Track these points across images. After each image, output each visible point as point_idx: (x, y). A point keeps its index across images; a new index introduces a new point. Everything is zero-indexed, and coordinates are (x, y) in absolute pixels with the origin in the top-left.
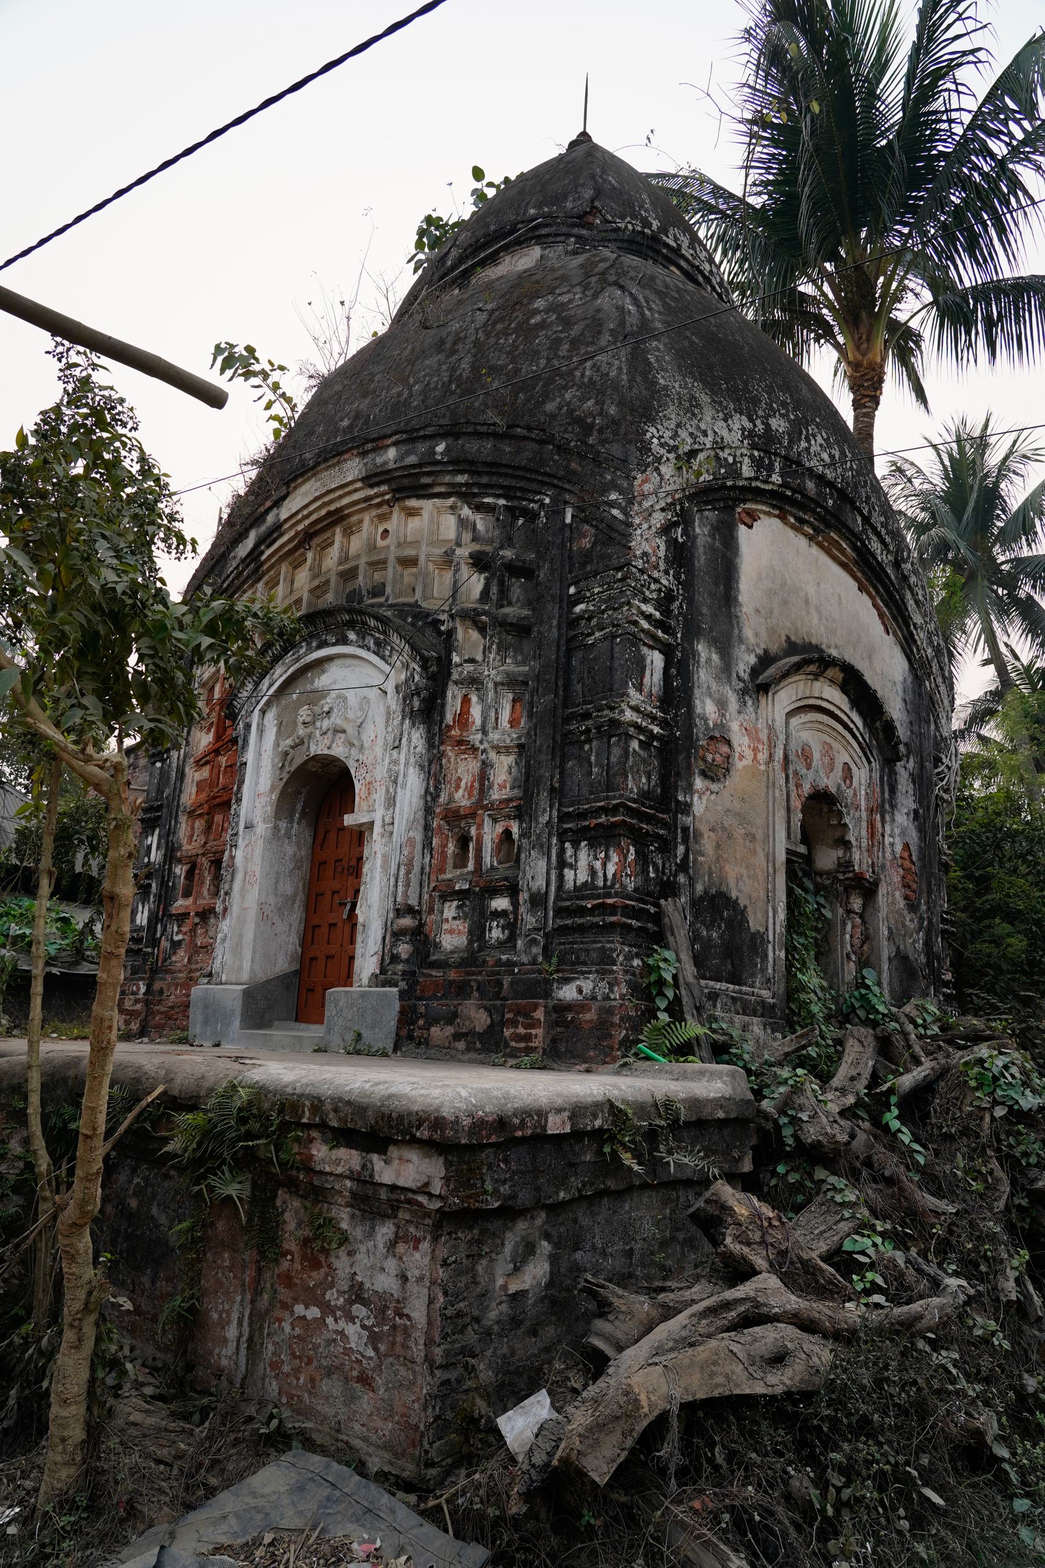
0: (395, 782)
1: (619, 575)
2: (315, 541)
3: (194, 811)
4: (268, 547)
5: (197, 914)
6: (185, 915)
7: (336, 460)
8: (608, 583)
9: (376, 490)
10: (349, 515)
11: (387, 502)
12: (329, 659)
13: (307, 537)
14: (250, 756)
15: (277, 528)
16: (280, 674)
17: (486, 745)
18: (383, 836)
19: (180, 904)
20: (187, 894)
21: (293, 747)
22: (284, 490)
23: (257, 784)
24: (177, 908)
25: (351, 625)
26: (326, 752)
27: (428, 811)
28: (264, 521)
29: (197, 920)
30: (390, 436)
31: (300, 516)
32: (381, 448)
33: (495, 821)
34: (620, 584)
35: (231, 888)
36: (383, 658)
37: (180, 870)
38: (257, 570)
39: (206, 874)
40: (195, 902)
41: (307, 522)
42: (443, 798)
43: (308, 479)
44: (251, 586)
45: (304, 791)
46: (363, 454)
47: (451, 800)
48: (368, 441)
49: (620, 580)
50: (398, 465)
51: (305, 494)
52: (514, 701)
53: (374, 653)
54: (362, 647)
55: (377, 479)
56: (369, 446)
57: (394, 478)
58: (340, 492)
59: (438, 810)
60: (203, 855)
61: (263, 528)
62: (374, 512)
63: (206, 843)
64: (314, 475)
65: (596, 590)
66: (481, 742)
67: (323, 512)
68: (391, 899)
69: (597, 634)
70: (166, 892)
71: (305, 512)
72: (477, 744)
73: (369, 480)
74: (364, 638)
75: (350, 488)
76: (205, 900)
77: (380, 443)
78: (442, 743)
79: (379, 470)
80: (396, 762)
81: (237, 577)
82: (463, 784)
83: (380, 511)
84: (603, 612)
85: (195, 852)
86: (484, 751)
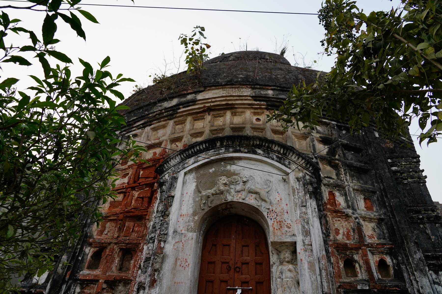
0: (308, 223)
1: (415, 160)
2: (212, 113)
3: (108, 217)
4: (184, 107)
5: (106, 282)
6: (94, 281)
7: (237, 86)
8: (410, 162)
9: (258, 102)
10: (236, 108)
11: (263, 109)
12: (240, 158)
13: (209, 110)
14: (177, 193)
15: (194, 102)
16: (202, 159)
17: (356, 215)
18: (306, 251)
19: (85, 273)
20: (90, 268)
21: (213, 195)
22: (203, 89)
23: (180, 209)
24: (84, 275)
25: (259, 147)
26: (241, 201)
27: (325, 242)
28: (186, 97)
29: (104, 286)
30: (271, 86)
31: (210, 100)
32: (264, 89)
33: (373, 254)
34: (415, 164)
35: (161, 267)
36: (284, 165)
37: (89, 251)
38: (172, 115)
39: (116, 256)
40: (104, 272)
41: (212, 104)
42: (332, 238)
43: (218, 89)
44: (166, 120)
45: (208, 219)
46: (253, 88)
47: (335, 240)
48: (257, 85)
49: (415, 162)
50: (274, 96)
51: (216, 93)
52: (365, 199)
53: (278, 161)
54: (268, 158)
55: (261, 99)
56: (258, 87)
57: (271, 101)
58: (238, 98)
59: (330, 243)
60: (116, 244)
61: (183, 100)
62: (253, 111)
63: (118, 237)
64: (223, 88)
65: (403, 163)
66: (353, 213)
67: (224, 103)
68: (320, 290)
69: (410, 180)
70: (75, 264)
71: (213, 100)
72: (350, 214)
73: (255, 98)
74: (269, 154)
75: (244, 98)
76: (114, 272)
77: (264, 87)
78: (324, 210)
79: (263, 96)
80: (306, 213)
81: (159, 114)
82: (341, 232)
83: (256, 111)
84: (410, 172)
85: (109, 241)
86: (356, 218)
